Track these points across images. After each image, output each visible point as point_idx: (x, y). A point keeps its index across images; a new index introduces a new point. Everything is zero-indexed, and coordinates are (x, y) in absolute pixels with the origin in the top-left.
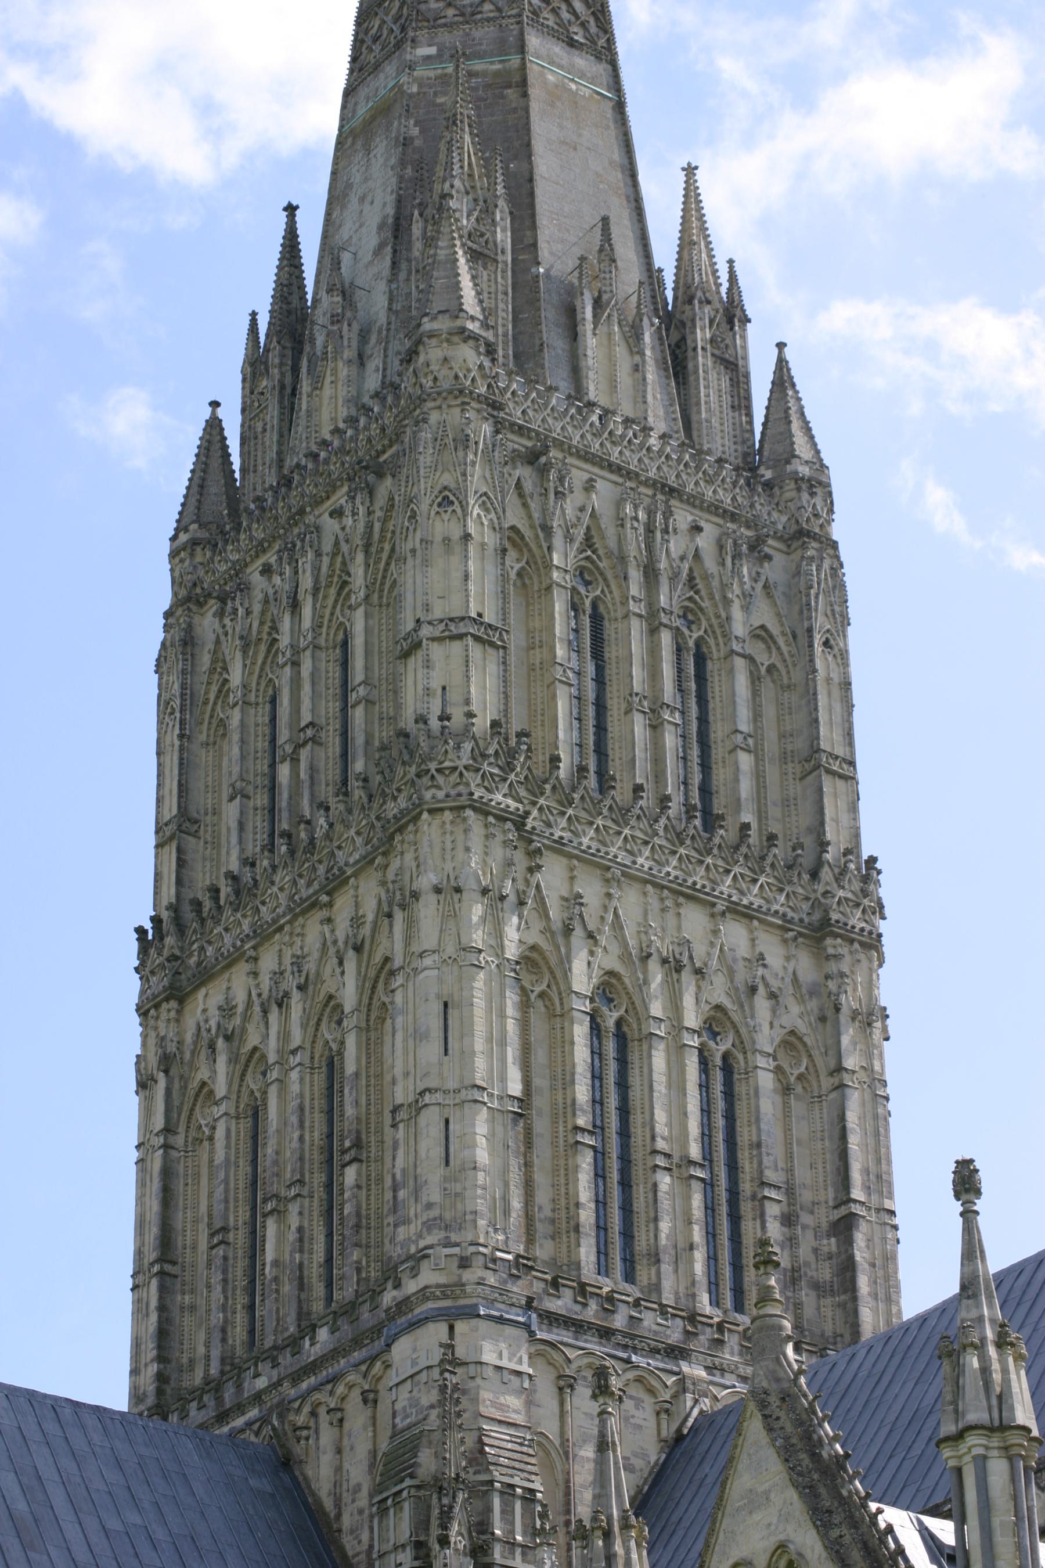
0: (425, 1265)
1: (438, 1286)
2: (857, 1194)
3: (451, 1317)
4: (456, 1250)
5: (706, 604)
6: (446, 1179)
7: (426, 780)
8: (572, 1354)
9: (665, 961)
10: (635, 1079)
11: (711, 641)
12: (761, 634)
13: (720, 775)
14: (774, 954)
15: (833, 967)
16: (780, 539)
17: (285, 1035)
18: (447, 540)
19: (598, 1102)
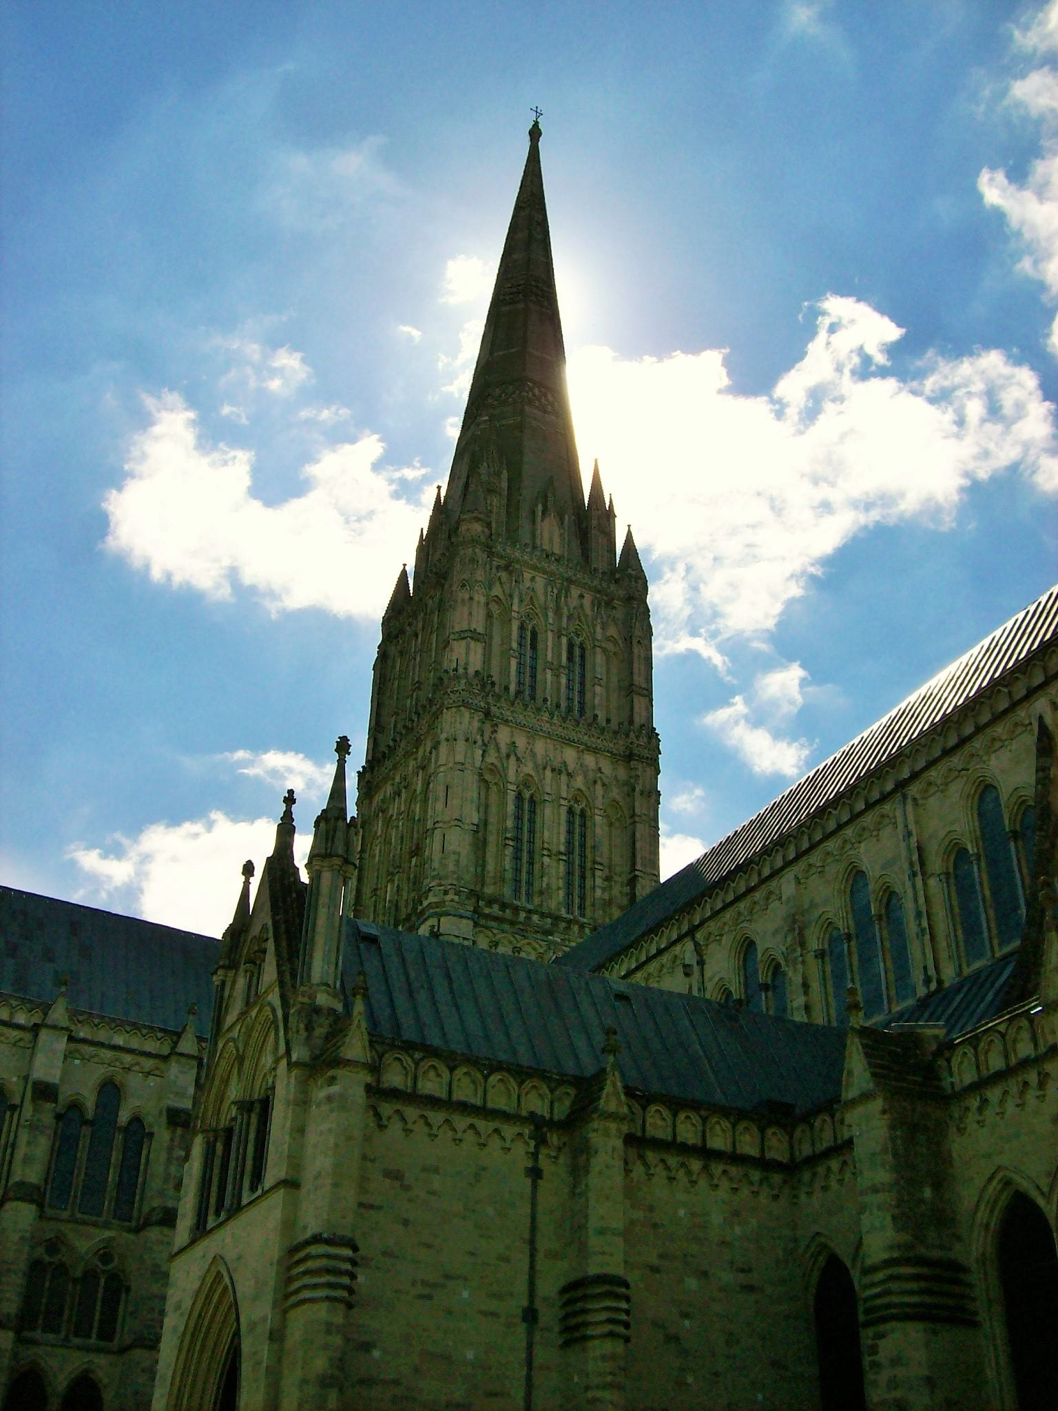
0: (431, 894)
1: (434, 903)
2: (638, 867)
3: (439, 915)
4: (442, 888)
5: (585, 627)
6: (442, 858)
7: (446, 696)
8: (495, 931)
9: (553, 770)
10: (538, 820)
11: (587, 642)
12: (610, 639)
13: (588, 696)
14: (607, 767)
15: (633, 773)
16: (622, 601)
17: (399, 808)
18: (463, 600)
19: (518, 828)
